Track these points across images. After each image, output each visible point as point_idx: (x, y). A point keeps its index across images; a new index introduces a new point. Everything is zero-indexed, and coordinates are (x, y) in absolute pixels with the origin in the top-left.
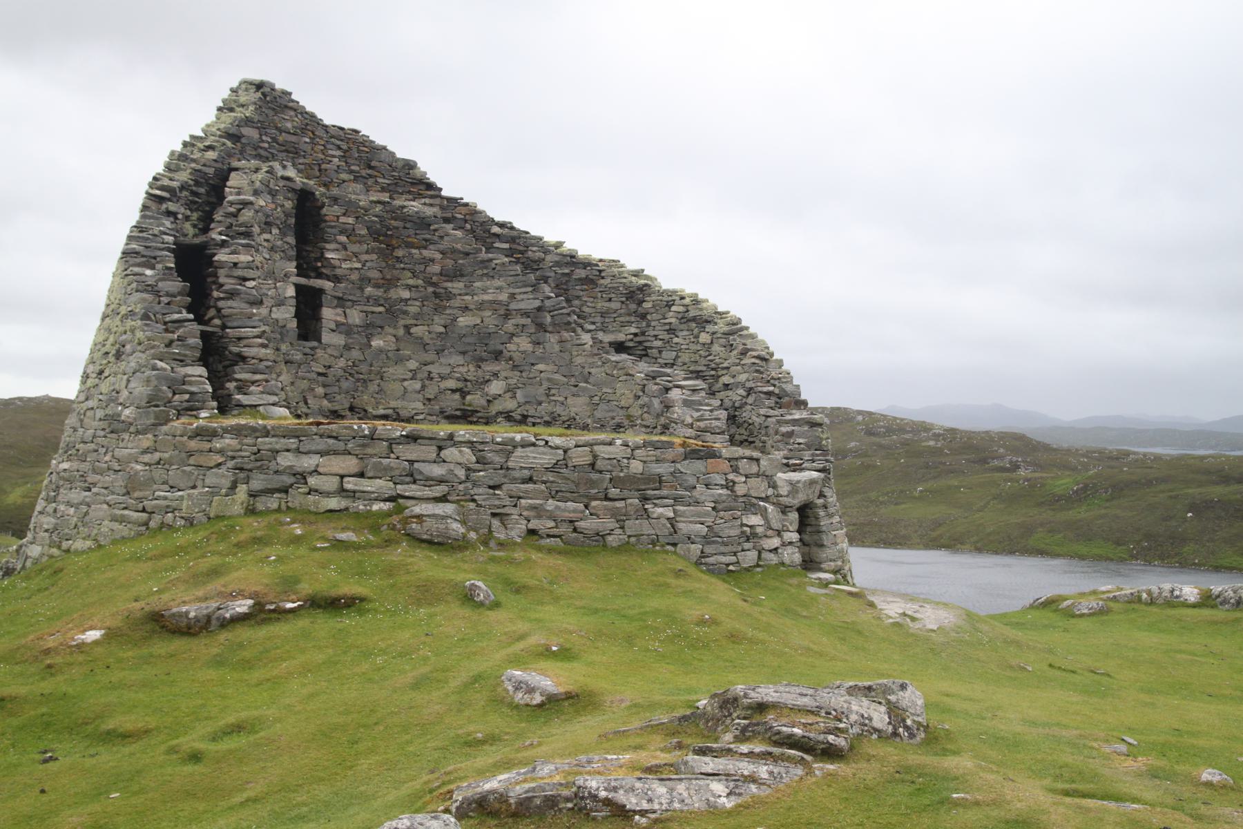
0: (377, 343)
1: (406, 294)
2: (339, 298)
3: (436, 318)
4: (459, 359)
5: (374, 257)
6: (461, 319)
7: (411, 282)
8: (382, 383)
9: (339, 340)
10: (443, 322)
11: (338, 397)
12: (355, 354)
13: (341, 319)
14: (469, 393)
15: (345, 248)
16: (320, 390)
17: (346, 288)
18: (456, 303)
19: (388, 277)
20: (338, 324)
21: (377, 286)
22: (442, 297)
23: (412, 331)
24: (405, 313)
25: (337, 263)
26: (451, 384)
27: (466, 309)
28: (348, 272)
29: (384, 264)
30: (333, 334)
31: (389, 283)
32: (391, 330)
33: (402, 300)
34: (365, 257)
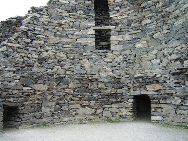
0: (138, 45)
1: (149, 21)
2: (119, 31)
3: (163, 27)
4: (177, 43)
5: (132, 11)
6: (176, 23)
7: (150, 15)
8: (141, 63)
9: (120, 47)
10: (167, 28)
11: (118, 71)
12: (128, 52)
13: (121, 39)
14: (185, 59)
15: (119, 11)
16: (109, 69)
17: (121, 27)
18: (172, 16)
19: (140, 16)
20: (119, 42)
21: (136, 22)
22: (164, 16)
23: (154, 36)
24: (151, 29)
25: (116, 18)
26: (174, 57)
27: (177, 17)
28: (122, 20)
29: (137, 12)
30: (116, 46)
31: (140, 20)
32: (144, 39)
33: (147, 24)
34: (129, 12)
